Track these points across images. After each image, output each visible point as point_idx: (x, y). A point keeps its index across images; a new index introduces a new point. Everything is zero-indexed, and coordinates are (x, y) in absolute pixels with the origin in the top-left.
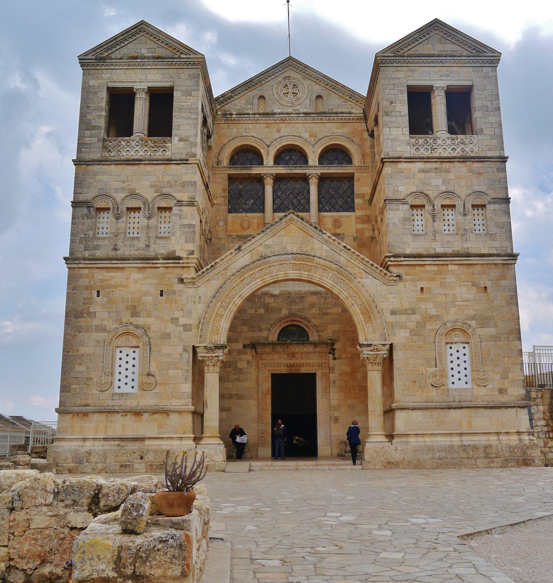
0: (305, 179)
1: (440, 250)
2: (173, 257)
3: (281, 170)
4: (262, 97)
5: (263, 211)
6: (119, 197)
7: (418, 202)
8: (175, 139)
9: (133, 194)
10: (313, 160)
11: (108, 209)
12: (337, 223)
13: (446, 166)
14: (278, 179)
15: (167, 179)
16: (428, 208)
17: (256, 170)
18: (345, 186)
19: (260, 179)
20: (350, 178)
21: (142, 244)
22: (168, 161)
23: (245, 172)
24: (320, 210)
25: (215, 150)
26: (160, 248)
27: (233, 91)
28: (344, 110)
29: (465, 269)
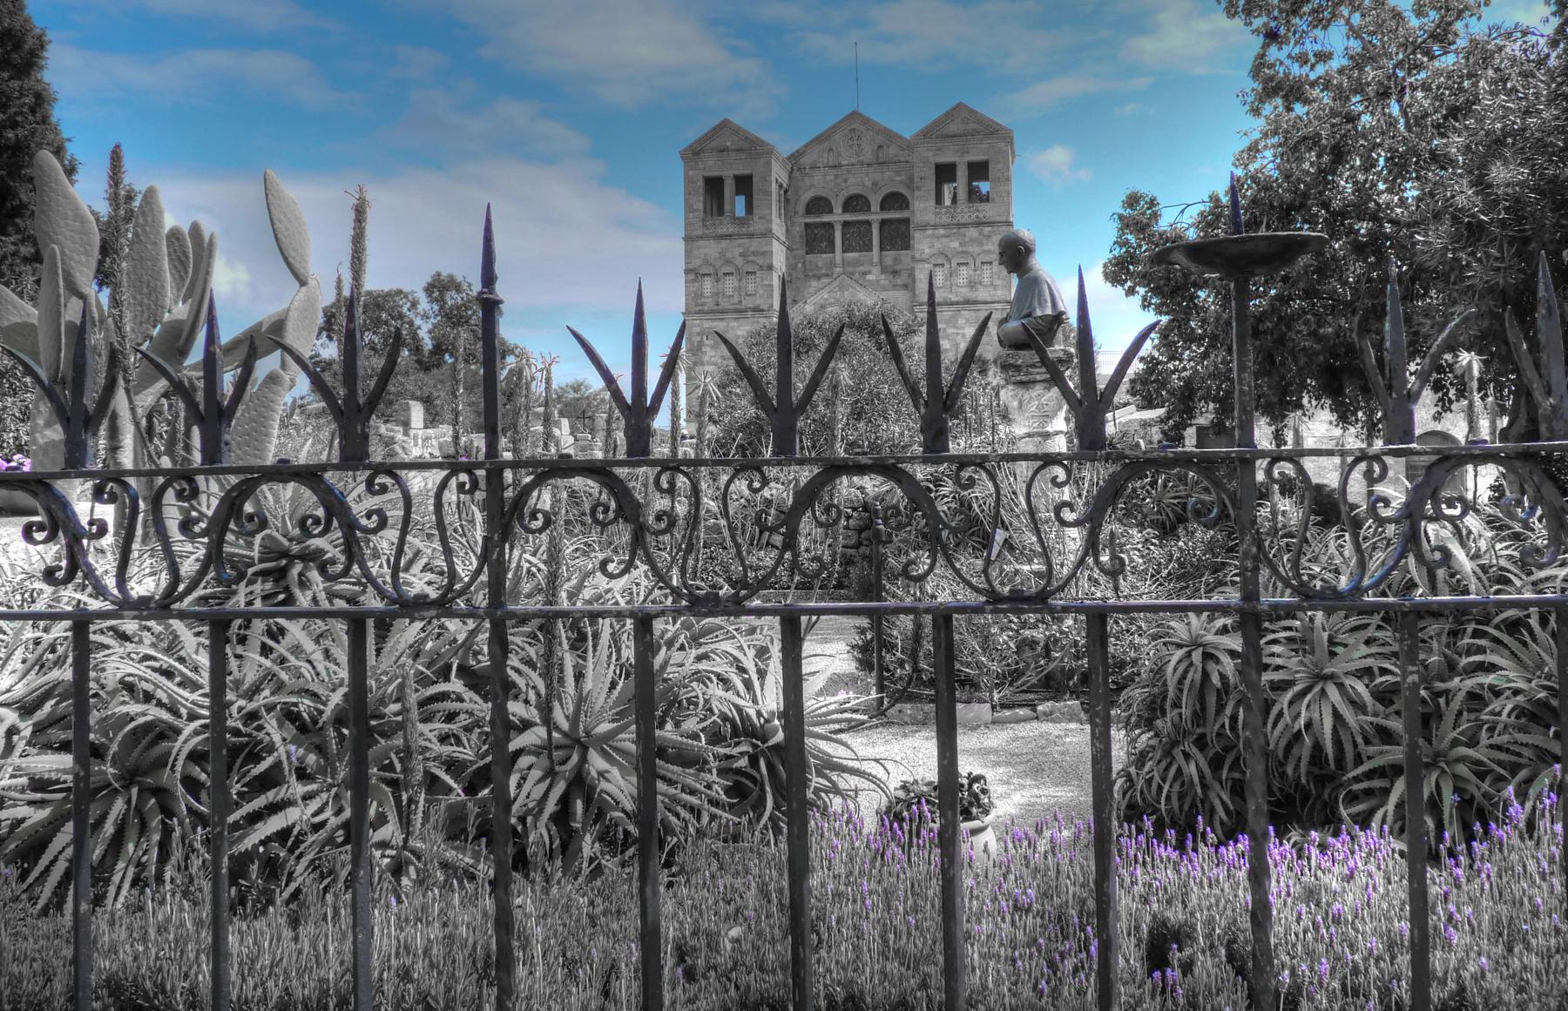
0: (868, 223)
1: (956, 299)
2: (757, 310)
3: (849, 217)
4: (831, 150)
5: (833, 252)
6: (719, 263)
7: (940, 261)
8: (756, 218)
9: (728, 262)
10: (875, 207)
11: (710, 274)
12: (897, 261)
13: (962, 230)
14: (846, 224)
15: (751, 249)
16: (947, 266)
17: (826, 218)
18: (903, 228)
19: (830, 226)
20: (907, 221)
21: (736, 300)
22: (751, 236)
23: (818, 220)
24: (881, 249)
25: (792, 202)
26: (748, 303)
27: (806, 146)
28: (902, 159)
29: (972, 313)
